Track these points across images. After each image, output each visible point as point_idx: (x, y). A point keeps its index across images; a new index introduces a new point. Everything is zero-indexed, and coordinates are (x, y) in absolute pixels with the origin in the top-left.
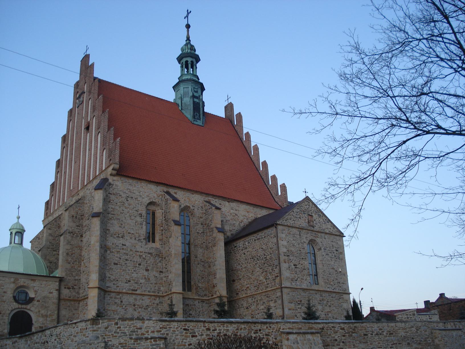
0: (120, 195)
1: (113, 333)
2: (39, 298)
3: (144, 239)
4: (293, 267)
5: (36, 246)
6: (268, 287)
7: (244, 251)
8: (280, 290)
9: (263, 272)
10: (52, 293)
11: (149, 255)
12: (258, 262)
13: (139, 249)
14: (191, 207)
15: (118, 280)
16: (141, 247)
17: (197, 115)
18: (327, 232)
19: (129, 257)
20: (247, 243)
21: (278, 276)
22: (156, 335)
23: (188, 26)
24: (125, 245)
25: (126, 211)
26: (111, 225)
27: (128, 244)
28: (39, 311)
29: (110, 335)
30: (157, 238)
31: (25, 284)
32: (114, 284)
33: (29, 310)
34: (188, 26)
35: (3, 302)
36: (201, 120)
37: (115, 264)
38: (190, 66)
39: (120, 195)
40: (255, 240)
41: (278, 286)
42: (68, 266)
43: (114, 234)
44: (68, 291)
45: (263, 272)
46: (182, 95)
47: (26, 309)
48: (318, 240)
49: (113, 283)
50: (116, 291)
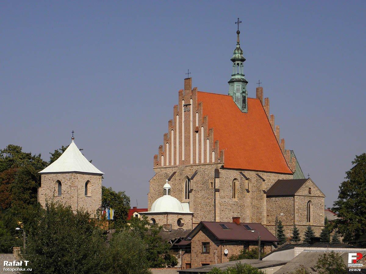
4: (300, 215)
5: (153, 184)
6: (287, 223)
14: (250, 178)
18: (317, 196)
23: (238, 33)
30: (236, 196)
34: (238, 33)
36: (246, 108)
48: (312, 200)
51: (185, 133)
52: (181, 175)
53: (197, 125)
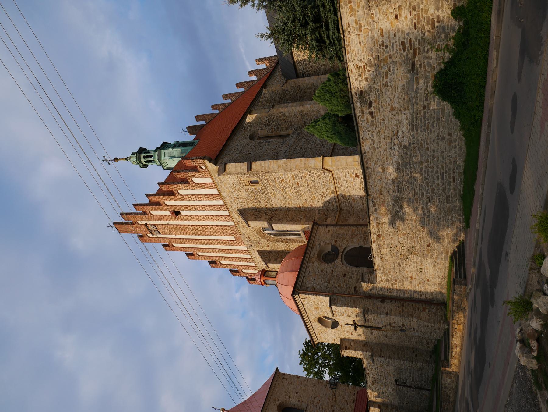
2: (333, 242)
10: (329, 231)
23: (116, 159)
28: (347, 241)
31: (316, 253)
33: (344, 249)
34: (116, 159)
35: (333, 272)
38: (147, 154)
47: (343, 252)
51: (191, 234)
52: (259, 244)
53: (168, 213)
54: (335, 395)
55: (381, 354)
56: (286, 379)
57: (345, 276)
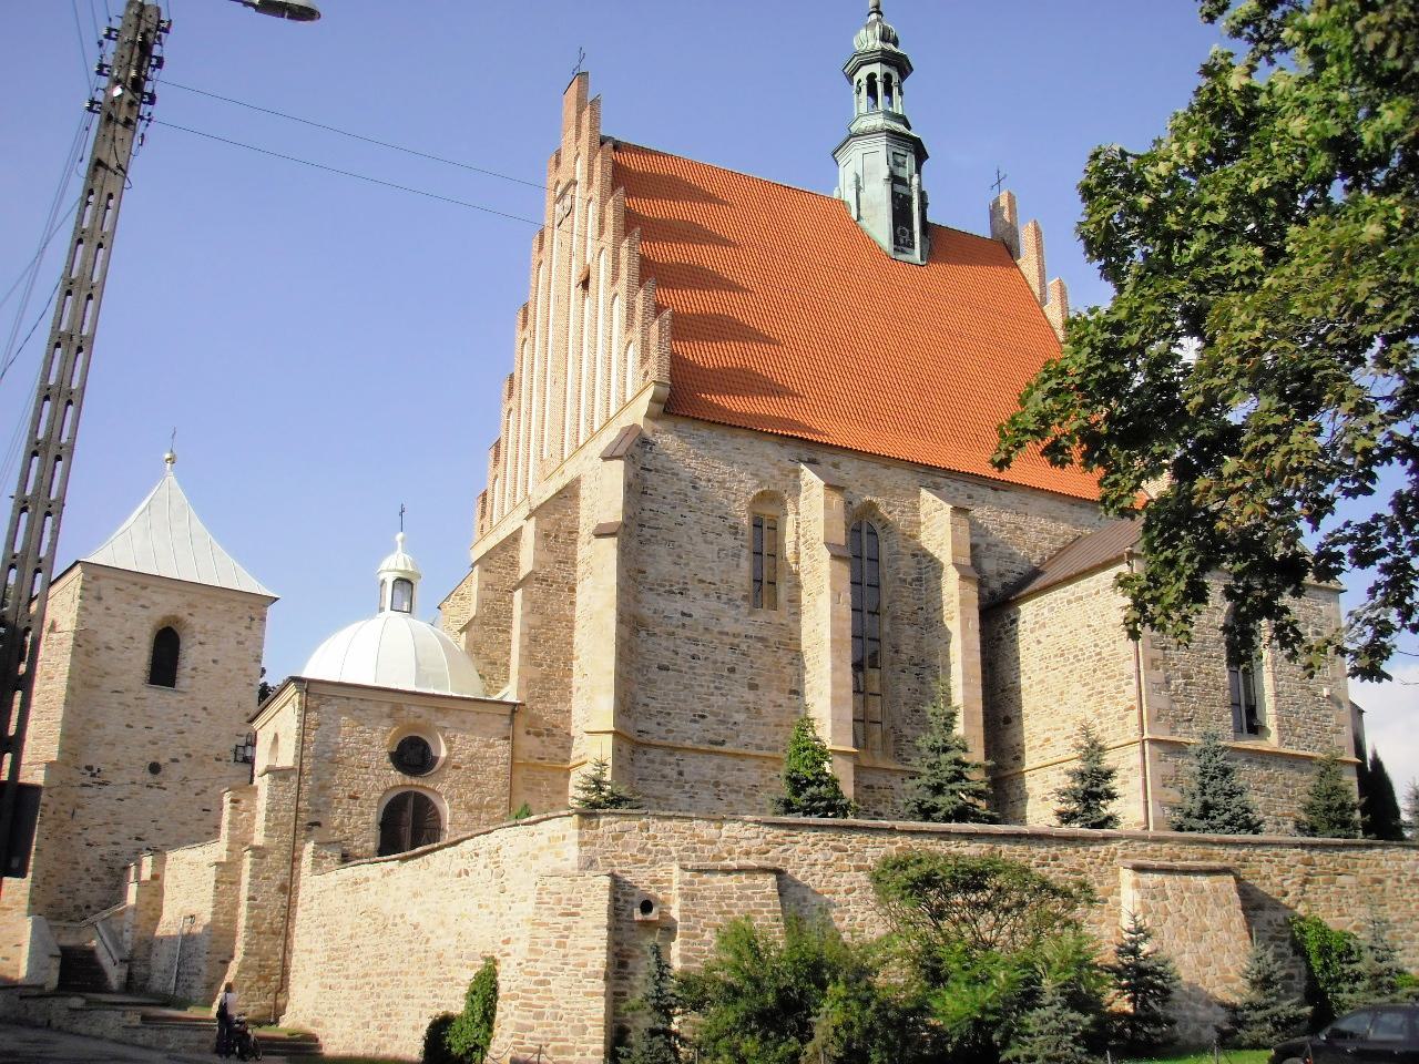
0: (673, 474)
1: (635, 851)
3: (745, 598)
7: (1037, 634)
8: (1138, 748)
9: (1091, 695)
11: (759, 645)
12: (1077, 665)
13: (730, 626)
15: (669, 714)
16: (737, 620)
17: (903, 233)
19: (700, 648)
20: (1045, 611)
21: (1132, 708)
22: (752, 862)
24: (690, 616)
25: (691, 517)
26: (650, 560)
27: (697, 613)
29: (626, 858)
31: (419, 721)
32: (659, 724)
33: (433, 791)
37: (662, 668)
38: (880, 88)
39: (673, 474)
40: (1069, 602)
41: (1132, 735)
42: (536, 673)
43: (659, 585)
44: (537, 741)
45: (1091, 695)
46: (860, 174)
49: (655, 720)
50: (663, 742)
54: (217, 760)
55: (224, 882)
56: (249, 628)
57: (354, 798)
